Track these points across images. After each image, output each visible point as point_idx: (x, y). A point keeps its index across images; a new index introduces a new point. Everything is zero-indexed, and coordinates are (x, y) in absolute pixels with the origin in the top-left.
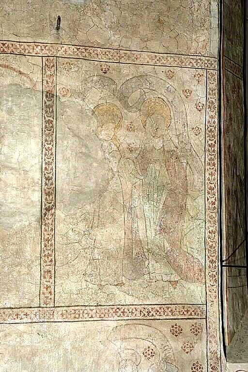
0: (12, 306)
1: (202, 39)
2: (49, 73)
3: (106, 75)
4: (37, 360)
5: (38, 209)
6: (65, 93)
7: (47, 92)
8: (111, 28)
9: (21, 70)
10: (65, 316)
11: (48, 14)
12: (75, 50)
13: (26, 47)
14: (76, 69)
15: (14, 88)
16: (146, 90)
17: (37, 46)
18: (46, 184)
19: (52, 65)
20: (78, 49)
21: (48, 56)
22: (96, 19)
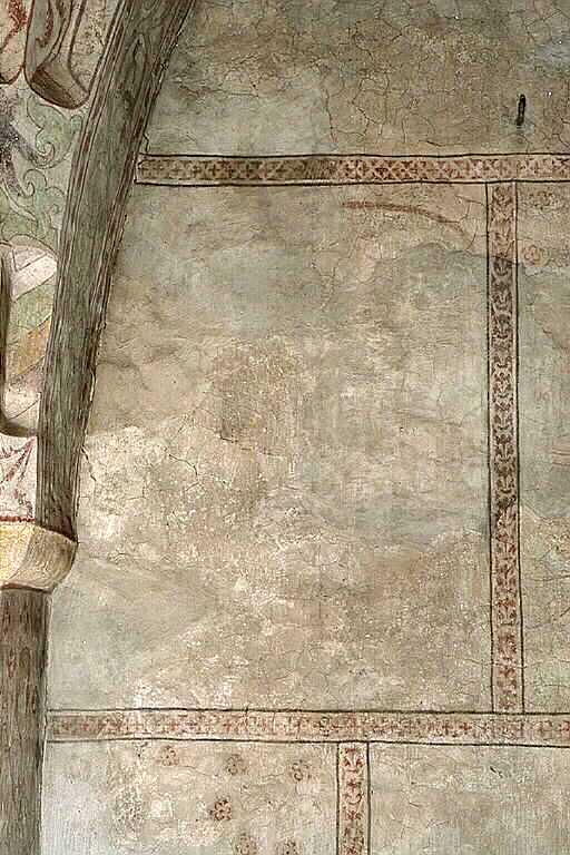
0: (434, 708)
2: (500, 216)
4: (492, 824)
5: (483, 503)
6: (536, 257)
7: (498, 258)
9: (443, 214)
10: (547, 736)
11: (497, 93)
12: (558, 163)
13: (453, 166)
15: (427, 251)
18: (498, 452)
19: (507, 199)
20: (563, 161)
21: (500, 182)
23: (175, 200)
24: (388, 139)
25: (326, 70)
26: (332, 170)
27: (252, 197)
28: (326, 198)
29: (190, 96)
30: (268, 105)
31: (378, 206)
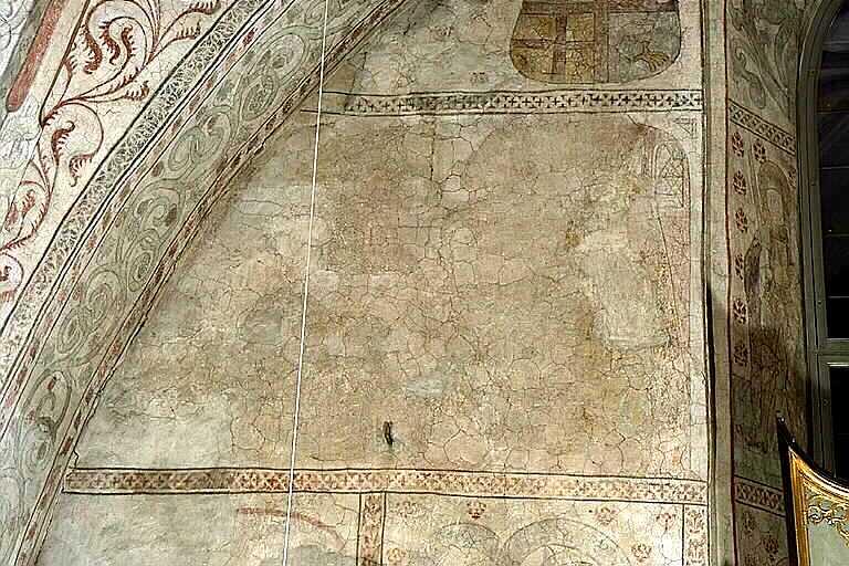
1: (672, 445)
2: (369, 522)
3: (477, 521)
6: (398, 559)
7: (365, 559)
8: (489, 434)
11: (374, 418)
12: (421, 477)
13: (334, 478)
14: (421, 513)
15: (307, 552)
16: (556, 548)
17: (352, 475)
19: (377, 507)
20: (425, 476)
21: (371, 492)
22: (463, 422)
23: (94, 505)
24: (279, 453)
25: (232, 397)
26: (231, 481)
27: (161, 503)
28: (222, 505)
29: (117, 418)
30: (183, 425)
31: (267, 512)
